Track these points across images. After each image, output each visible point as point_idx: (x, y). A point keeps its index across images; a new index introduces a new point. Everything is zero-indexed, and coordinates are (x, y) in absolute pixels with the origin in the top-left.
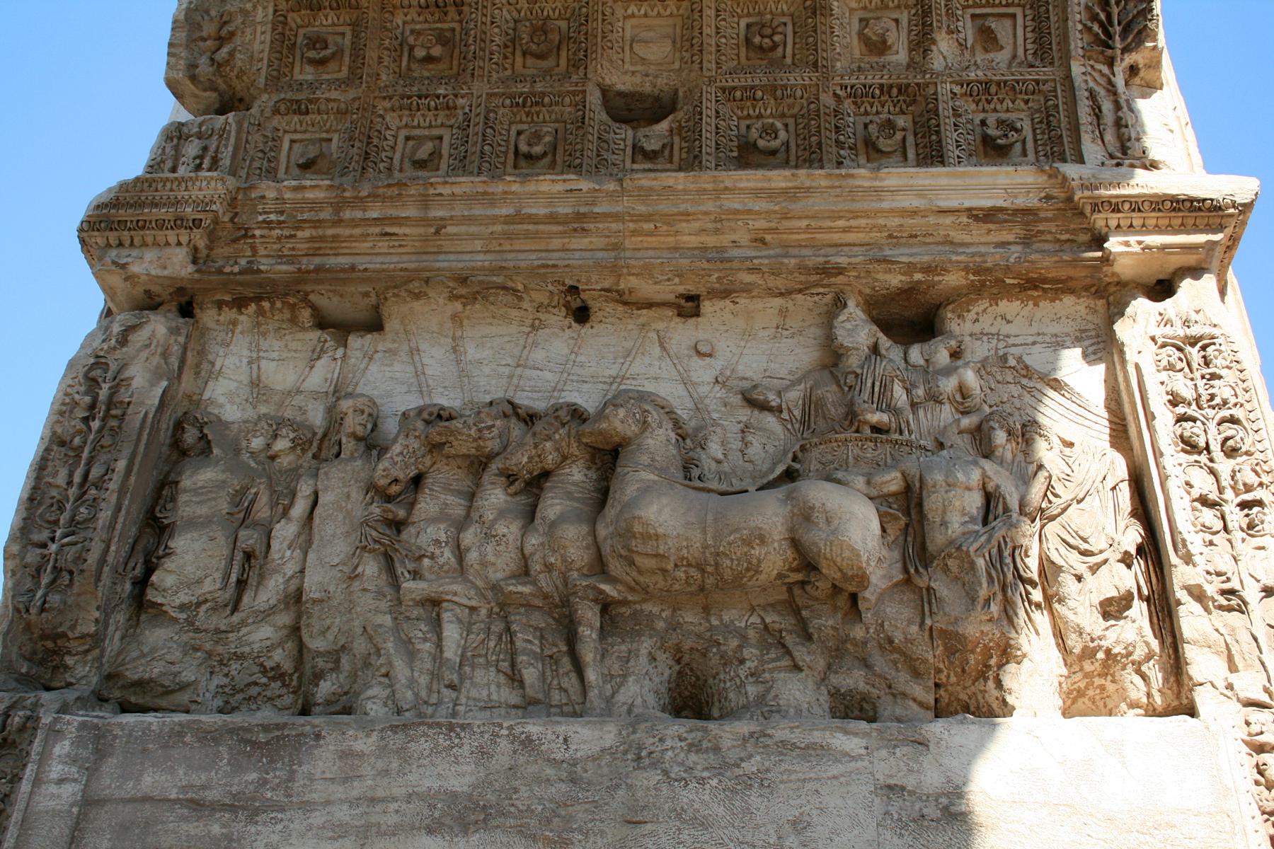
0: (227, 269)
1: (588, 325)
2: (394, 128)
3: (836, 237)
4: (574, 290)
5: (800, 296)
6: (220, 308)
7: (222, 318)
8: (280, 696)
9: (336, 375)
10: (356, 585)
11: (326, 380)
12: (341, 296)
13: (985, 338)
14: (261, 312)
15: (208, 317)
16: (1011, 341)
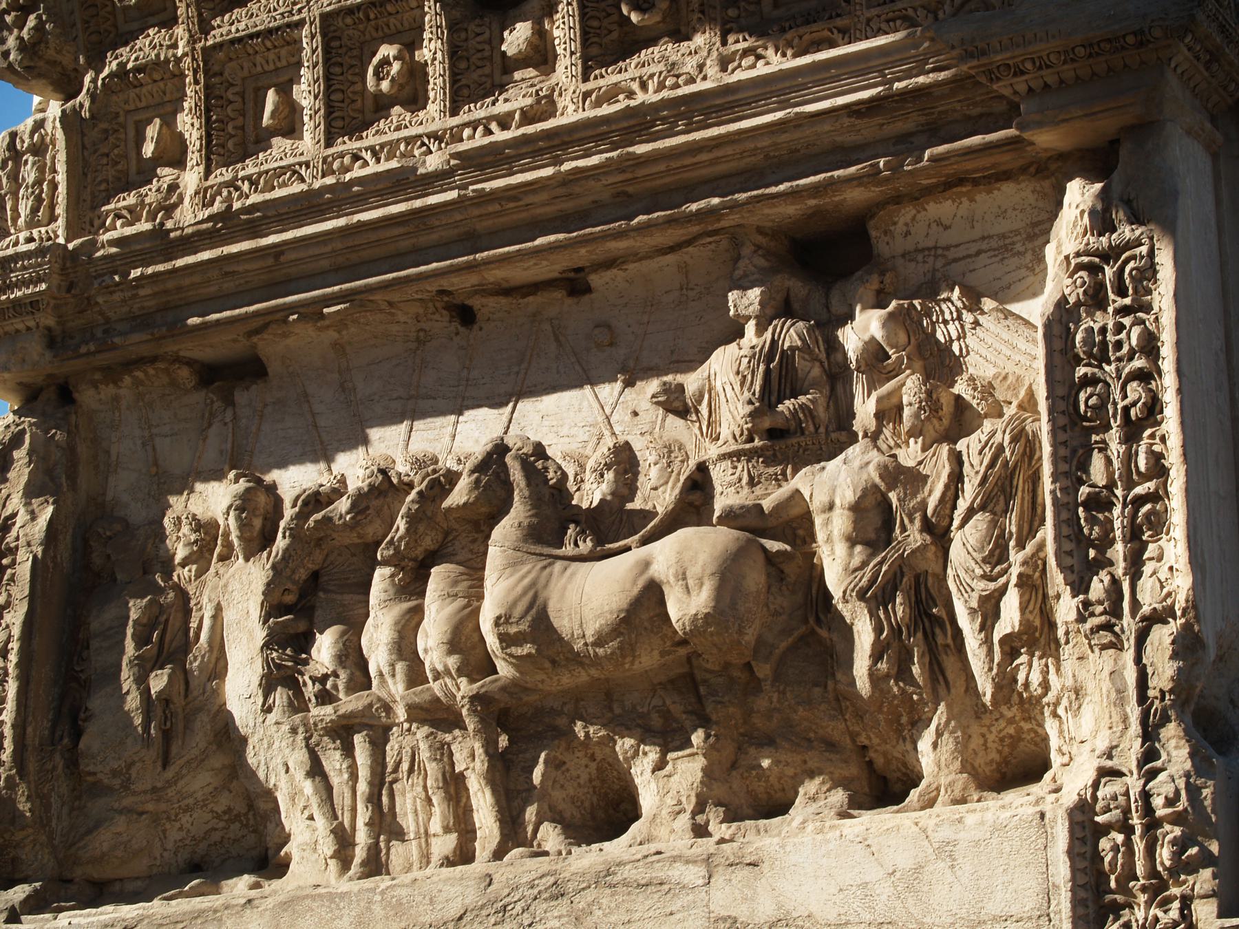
0: (83, 350)
1: (476, 327)
2: (239, 82)
3: (705, 172)
4: (442, 292)
5: (690, 249)
6: (97, 388)
7: (102, 396)
8: (243, 837)
9: (229, 446)
10: (272, 718)
11: (221, 452)
12: (212, 346)
13: (920, 258)
14: (137, 383)
15: (87, 397)
16: (952, 254)
